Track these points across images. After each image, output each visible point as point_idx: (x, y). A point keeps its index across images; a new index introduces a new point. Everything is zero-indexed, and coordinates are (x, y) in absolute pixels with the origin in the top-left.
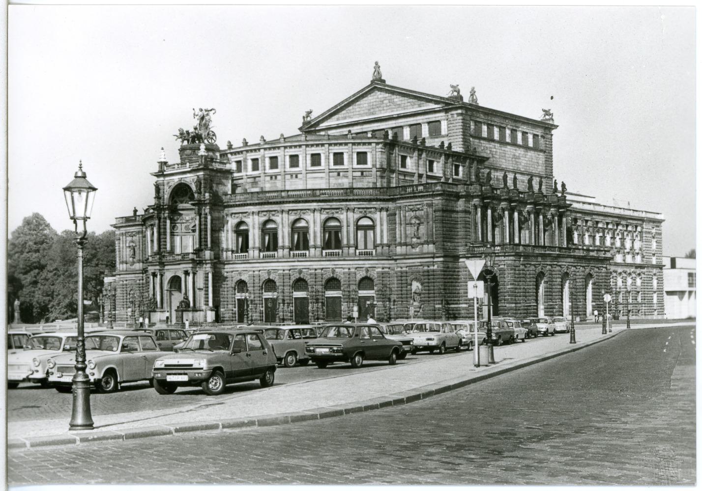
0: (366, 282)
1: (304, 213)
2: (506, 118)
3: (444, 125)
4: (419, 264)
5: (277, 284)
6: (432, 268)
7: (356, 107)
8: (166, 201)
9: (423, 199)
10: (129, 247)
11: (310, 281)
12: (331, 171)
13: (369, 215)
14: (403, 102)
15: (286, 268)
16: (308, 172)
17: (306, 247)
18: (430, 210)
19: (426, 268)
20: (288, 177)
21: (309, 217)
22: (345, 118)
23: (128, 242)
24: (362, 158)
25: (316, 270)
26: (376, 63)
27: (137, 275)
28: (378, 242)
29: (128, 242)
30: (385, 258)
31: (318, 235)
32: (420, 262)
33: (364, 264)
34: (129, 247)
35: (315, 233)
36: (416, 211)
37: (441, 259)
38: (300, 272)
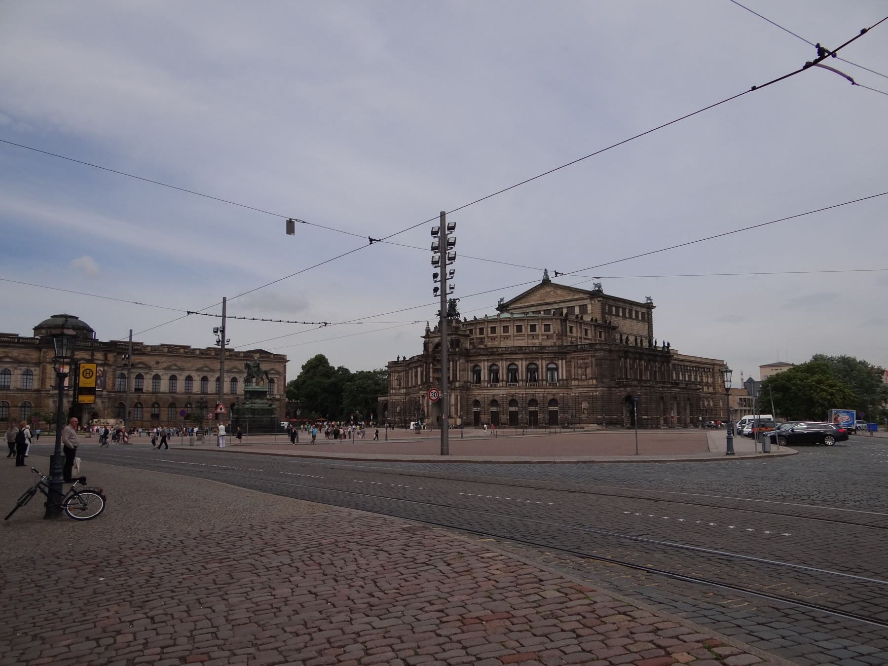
0: (553, 402)
2: (627, 303)
3: (589, 307)
5: (499, 402)
6: (595, 394)
8: (430, 353)
10: (397, 379)
11: (520, 401)
12: (528, 335)
13: (554, 362)
16: (514, 336)
17: (516, 381)
18: (593, 359)
20: (503, 339)
21: (519, 363)
22: (525, 303)
24: (547, 328)
25: (523, 394)
26: (546, 270)
28: (560, 378)
31: (524, 373)
35: (522, 372)
38: (513, 395)
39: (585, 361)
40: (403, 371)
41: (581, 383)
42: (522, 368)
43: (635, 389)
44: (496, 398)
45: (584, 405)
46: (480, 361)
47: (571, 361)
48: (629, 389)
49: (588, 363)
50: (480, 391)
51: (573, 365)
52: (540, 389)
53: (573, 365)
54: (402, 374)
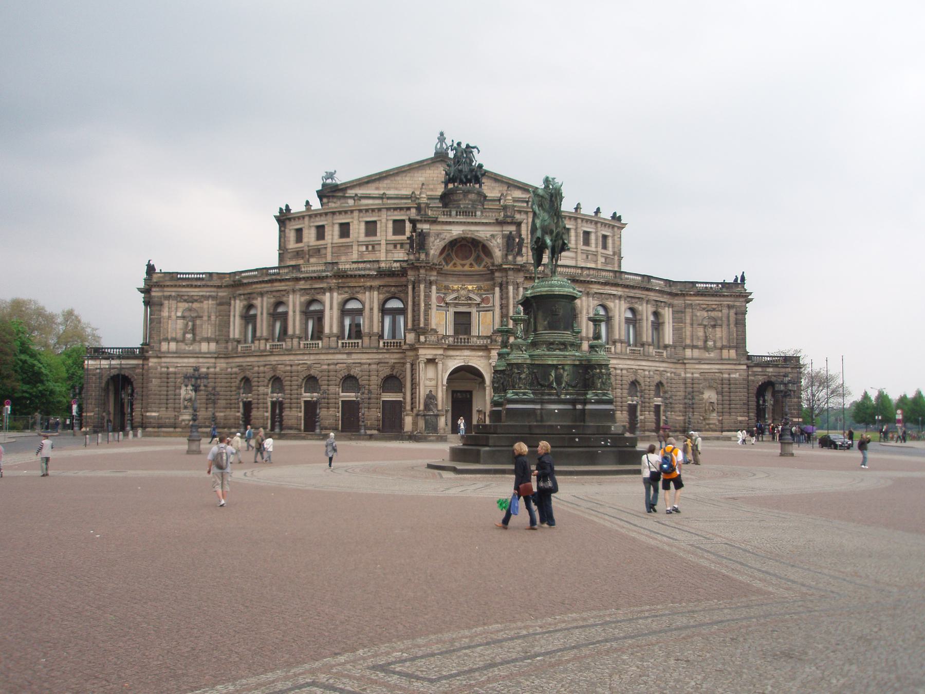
1: (607, 299)
4: (717, 371)
6: (733, 376)
7: (407, 178)
9: (722, 299)
10: (183, 317)
12: (583, 252)
13: (660, 310)
18: (732, 312)
19: (726, 376)
22: (389, 189)
26: (442, 134)
27: (201, 360)
30: (675, 361)
34: (183, 317)
37: (745, 367)
39: (713, 314)
41: (707, 355)
42: (620, 316)
43: (783, 370)
45: (710, 395)
47: (684, 312)
48: (771, 370)
51: (688, 321)
53: (688, 321)
54: (208, 304)
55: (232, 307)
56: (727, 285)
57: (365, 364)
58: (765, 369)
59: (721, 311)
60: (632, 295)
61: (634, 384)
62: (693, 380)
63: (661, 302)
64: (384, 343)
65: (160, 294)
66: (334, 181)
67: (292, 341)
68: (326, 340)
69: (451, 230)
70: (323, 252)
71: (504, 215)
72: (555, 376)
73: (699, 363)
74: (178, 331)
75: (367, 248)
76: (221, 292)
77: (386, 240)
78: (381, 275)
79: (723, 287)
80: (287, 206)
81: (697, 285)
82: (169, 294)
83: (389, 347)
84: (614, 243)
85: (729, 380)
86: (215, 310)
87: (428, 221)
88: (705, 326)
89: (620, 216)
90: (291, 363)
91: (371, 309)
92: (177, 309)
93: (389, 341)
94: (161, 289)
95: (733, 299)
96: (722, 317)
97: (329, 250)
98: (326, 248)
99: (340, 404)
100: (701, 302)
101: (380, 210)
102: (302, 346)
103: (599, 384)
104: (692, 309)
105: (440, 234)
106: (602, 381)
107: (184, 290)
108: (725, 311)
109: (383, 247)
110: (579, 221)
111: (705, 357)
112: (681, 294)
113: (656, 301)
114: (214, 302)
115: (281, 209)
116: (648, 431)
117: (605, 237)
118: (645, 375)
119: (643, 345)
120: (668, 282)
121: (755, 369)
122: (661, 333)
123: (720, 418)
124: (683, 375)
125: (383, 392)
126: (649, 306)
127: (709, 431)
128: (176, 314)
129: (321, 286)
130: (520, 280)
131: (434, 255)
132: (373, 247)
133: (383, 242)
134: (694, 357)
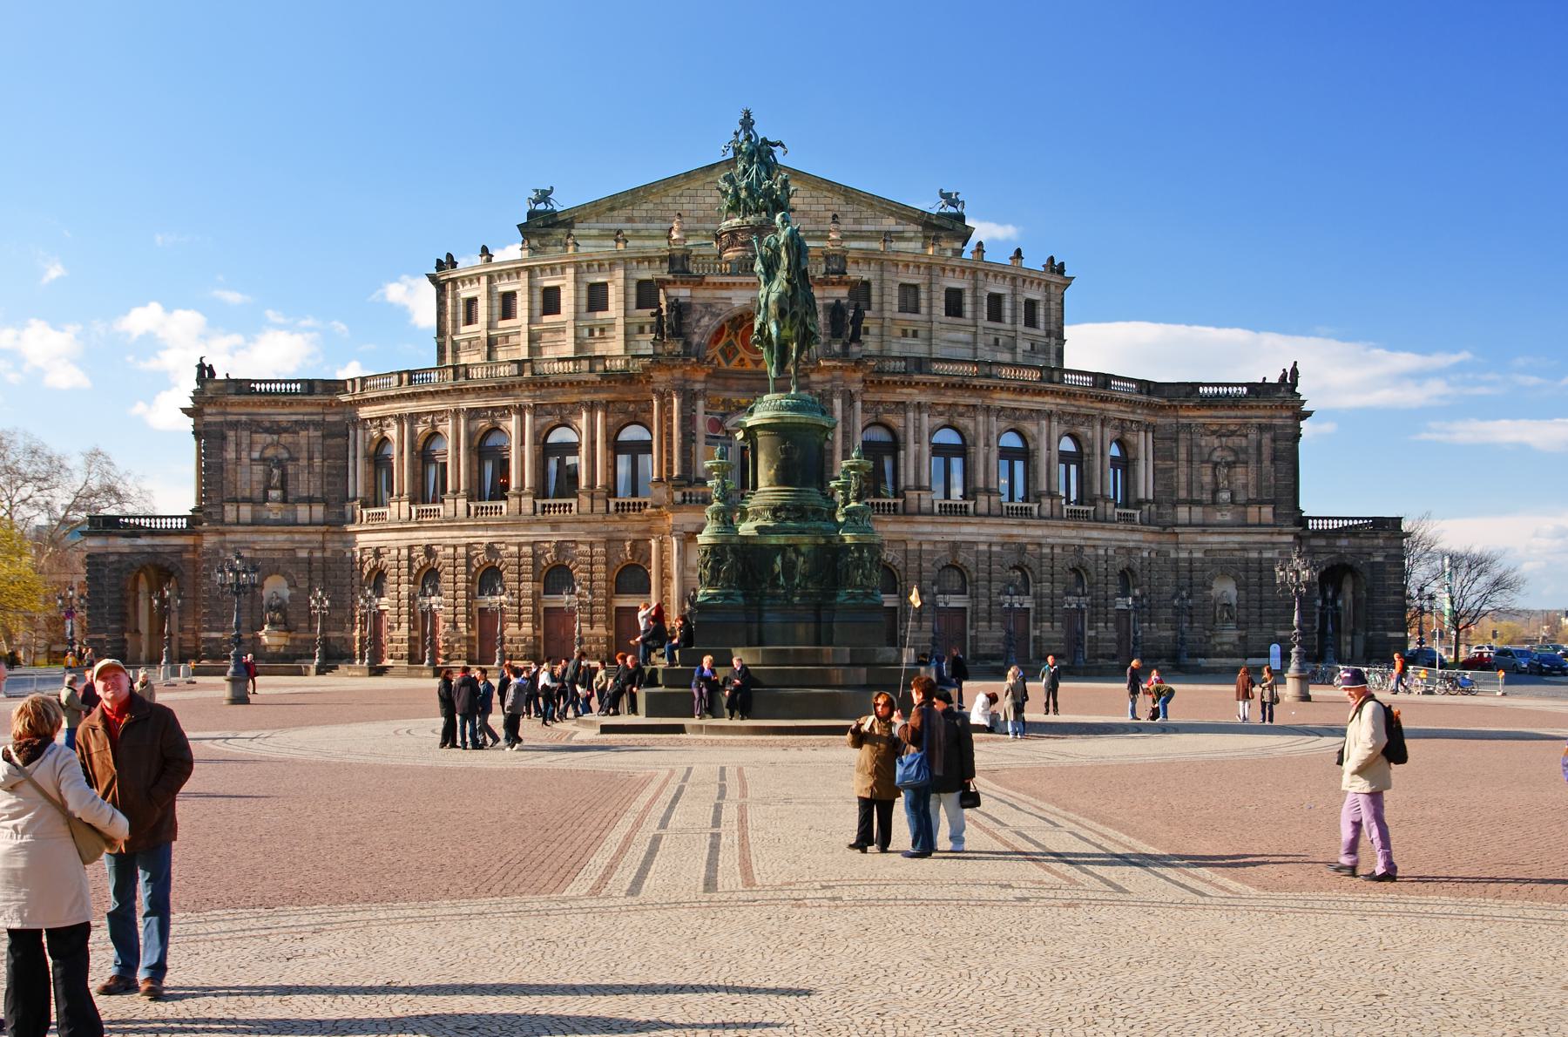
1: (1025, 418)
4: (1237, 546)
5: (974, 575)
9: (1248, 413)
13: (1128, 436)
14: (814, 208)
15: (995, 539)
18: (1266, 438)
19: (1254, 555)
20: (899, 333)
22: (650, 220)
23: (258, 448)
26: (748, 114)
27: (297, 537)
29: (258, 448)
32: (1239, 543)
33: (1127, 541)
34: (263, 460)
36: (1229, 436)
38: (1022, 548)
40: (304, 425)
42: (1049, 449)
43: (1366, 542)
44: (962, 557)
45: (1226, 590)
46: (902, 406)
47: (1176, 440)
48: (1343, 542)
49: (1245, 450)
50: (905, 528)
51: (1183, 455)
52: (1103, 528)
55: (351, 442)
56: (1258, 389)
57: (582, 543)
58: (1332, 541)
59: (1246, 436)
60: (1073, 410)
61: (1078, 571)
62: (1191, 564)
63: (1132, 422)
64: (617, 504)
65: (219, 419)
66: (550, 207)
67: (455, 503)
68: (514, 501)
69: (730, 299)
70: (513, 339)
71: (827, 269)
72: (782, 564)
73: (1204, 532)
74: (255, 485)
75: (591, 333)
76: (332, 414)
77: (625, 316)
78: (609, 382)
79: (1249, 391)
80: (449, 256)
81: (1201, 389)
82: (235, 418)
83: (626, 512)
84: (1047, 315)
85: (1260, 563)
86: (320, 447)
87: (688, 283)
88: (1216, 465)
89: (1062, 264)
90: (454, 542)
91: (593, 443)
92: (251, 445)
93: (626, 501)
94: (220, 410)
95: (1269, 413)
96: (1247, 447)
97: (524, 337)
98: (518, 333)
99: (542, 614)
100: (1208, 421)
101: (612, 265)
102: (472, 511)
103: (858, 579)
104: (1191, 433)
105: (711, 305)
106: (863, 573)
107: (263, 410)
108: (1253, 435)
109: (619, 332)
110: (981, 275)
111: (1215, 522)
112: (1170, 407)
113: (1122, 420)
114: (319, 433)
115: (439, 261)
116: (1103, 656)
117: (1031, 305)
118: (1097, 555)
119: (1093, 502)
120: (1146, 386)
121: (1314, 542)
122: (1131, 475)
123: (1244, 633)
124: (1173, 555)
125: (616, 593)
126: (1107, 430)
127: (1221, 657)
128: (250, 454)
129: (505, 403)
130: (856, 387)
131: (699, 344)
132: (602, 330)
133: (620, 322)
134: (1194, 521)
